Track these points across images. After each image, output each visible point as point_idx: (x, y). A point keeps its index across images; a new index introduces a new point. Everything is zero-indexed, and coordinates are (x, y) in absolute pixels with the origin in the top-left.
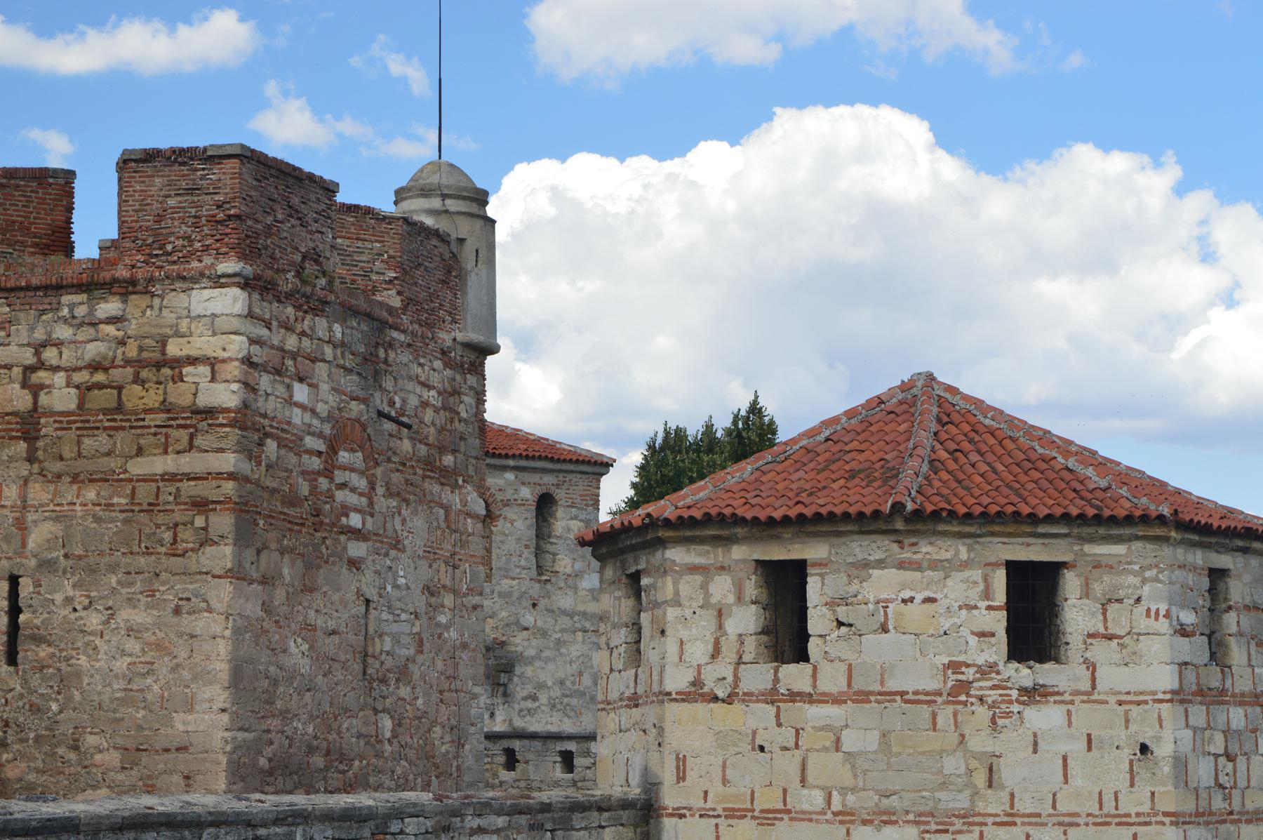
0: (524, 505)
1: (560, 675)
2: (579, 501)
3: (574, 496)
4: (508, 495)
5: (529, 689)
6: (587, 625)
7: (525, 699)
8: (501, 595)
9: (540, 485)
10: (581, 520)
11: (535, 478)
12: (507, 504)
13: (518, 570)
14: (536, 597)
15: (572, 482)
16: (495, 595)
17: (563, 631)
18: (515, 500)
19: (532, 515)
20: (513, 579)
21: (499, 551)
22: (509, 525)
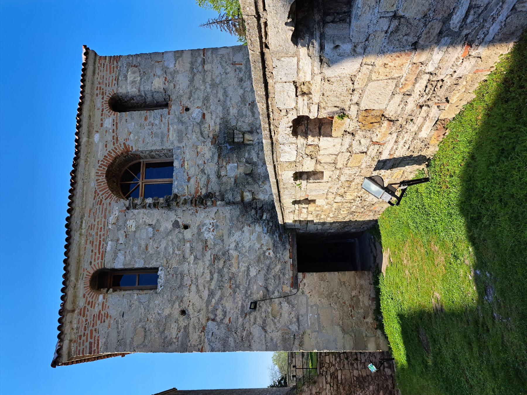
0: (117, 123)
1: (234, 82)
2: (114, 74)
3: (111, 79)
4: (109, 138)
5: (246, 110)
6: (200, 60)
8: (180, 141)
9: (103, 111)
10: (128, 70)
11: (98, 113)
12: (116, 139)
13: (163, 126)
14: (181, 108)
15: (101, 81)
16: (181, 145)
17: (204, 81)
18: (113, 132)
19: (126, 115)
22: (132, 135)
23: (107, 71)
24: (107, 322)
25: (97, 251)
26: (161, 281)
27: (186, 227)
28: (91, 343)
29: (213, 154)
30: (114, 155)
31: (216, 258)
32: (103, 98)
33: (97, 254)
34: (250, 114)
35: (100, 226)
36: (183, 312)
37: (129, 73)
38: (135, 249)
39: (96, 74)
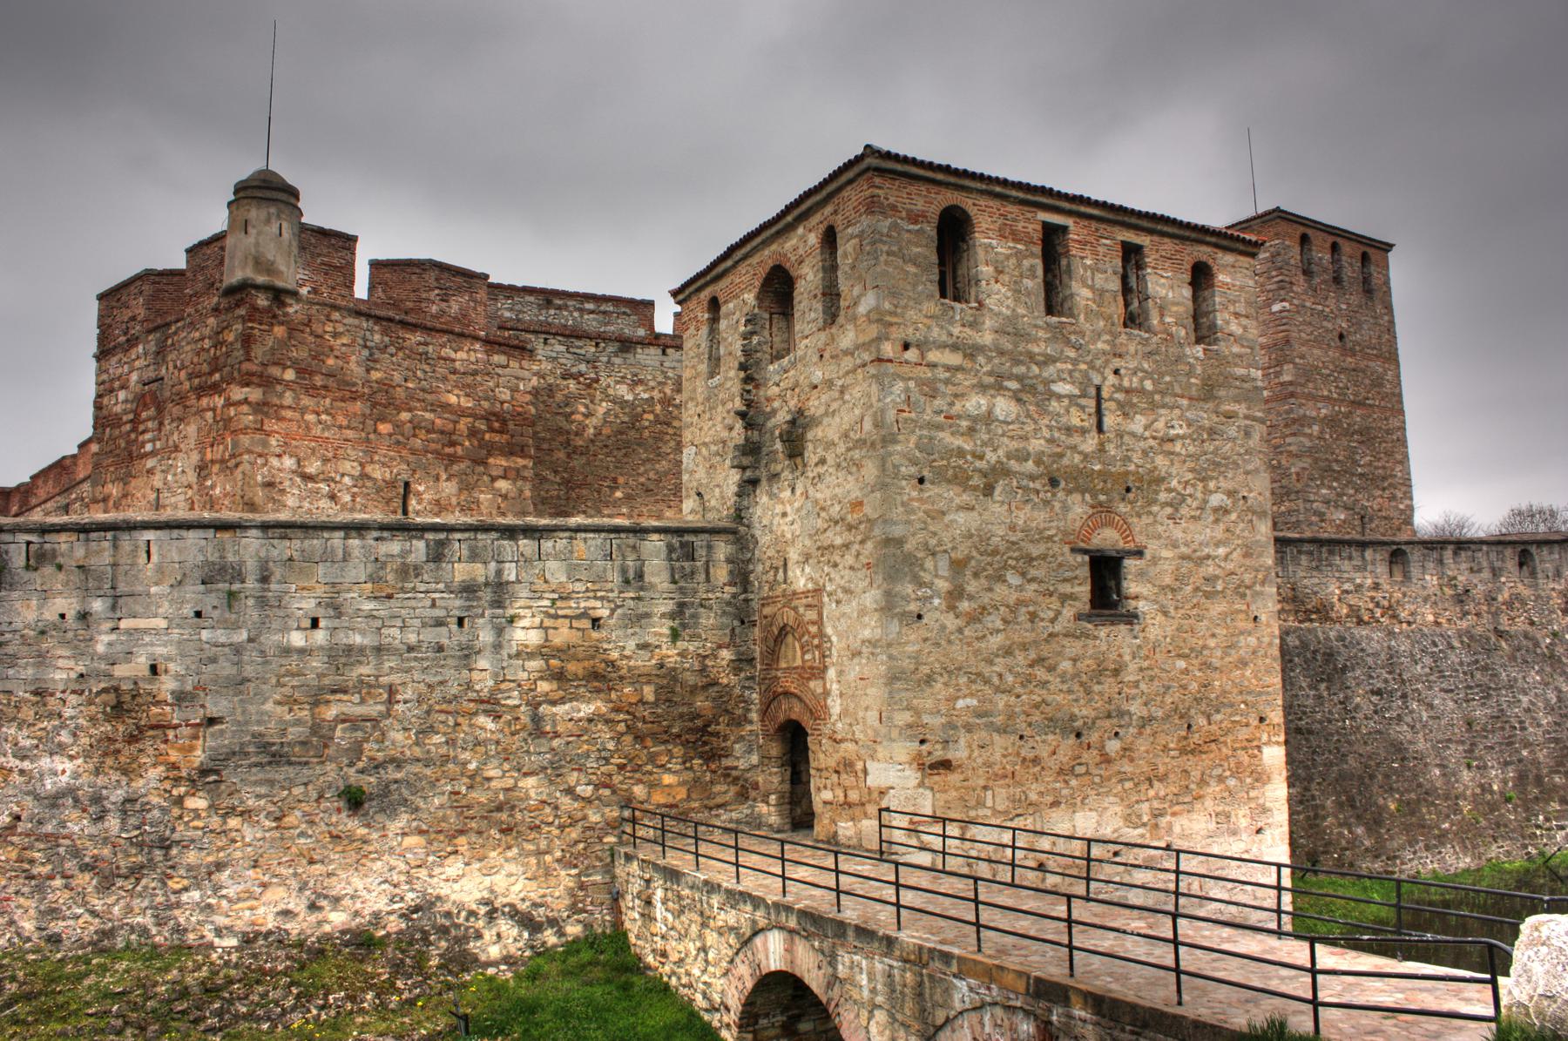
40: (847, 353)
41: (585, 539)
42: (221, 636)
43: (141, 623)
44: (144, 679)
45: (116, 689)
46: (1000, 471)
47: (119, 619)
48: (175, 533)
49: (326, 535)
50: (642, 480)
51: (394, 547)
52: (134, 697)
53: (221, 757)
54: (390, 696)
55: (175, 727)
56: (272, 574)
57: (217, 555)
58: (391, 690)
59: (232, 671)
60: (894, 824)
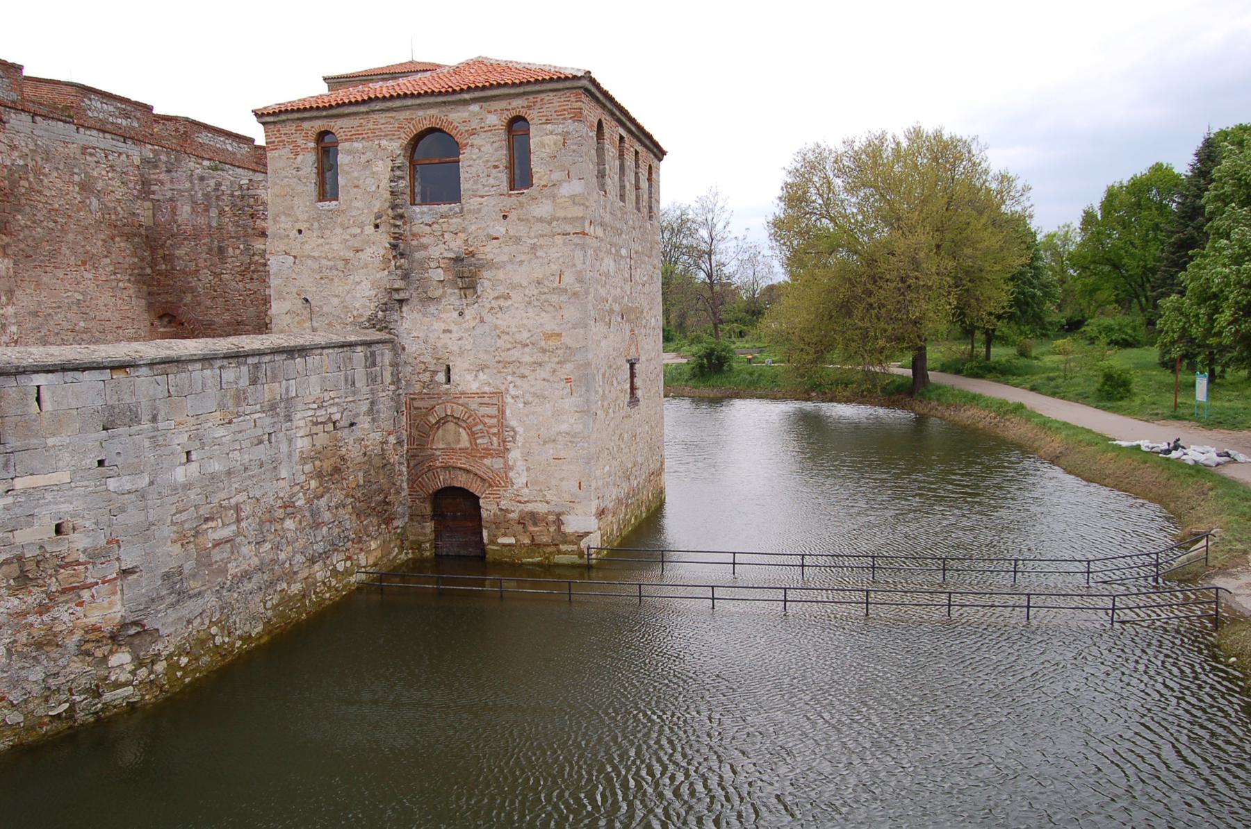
1: (538, 274)
3: (548, 114)
4: (475, 124)
5: (501, 289)
7: (497, 298)
11: (503, 104)
12: (473, 133)
15: (545, 101)
20: (482, 197)
21: (466, 175)
23: (560, 106)
24: (292, 156)
25: (353, 133)
26: (326, 205)
27: (377, 226)
28: (274, 142)
29: (454, 252)
30: (453, 133)
31: (346, 261)
32: (523, 107)
33: (350, 133)
34: (496, 295)
35: (376, 131)
36: (300, 232)
37: (555, 137)
38: (356, 174)
39: (554, 94)
40: (540, 220)
41: (327, 354)
42: (126, 483)
43: (39, 480)
44: (50, 540)
45: (20, 558)
46: (611, 311)
47: (12, 479)
48: (70, 376)
49: (190, 368)
50: (22, 246)
51: (229, 374)
52: (38, 563)
53: (142, 607)
54: (238, 515)
55: (89, 587)
56: (158, 411)
57: (115, 397)
58: (238, 508)
59: (140, 517)
60: (673, 559)
